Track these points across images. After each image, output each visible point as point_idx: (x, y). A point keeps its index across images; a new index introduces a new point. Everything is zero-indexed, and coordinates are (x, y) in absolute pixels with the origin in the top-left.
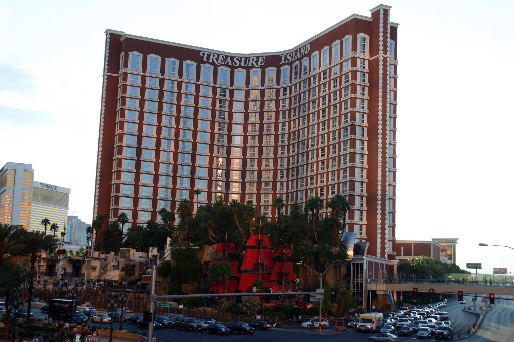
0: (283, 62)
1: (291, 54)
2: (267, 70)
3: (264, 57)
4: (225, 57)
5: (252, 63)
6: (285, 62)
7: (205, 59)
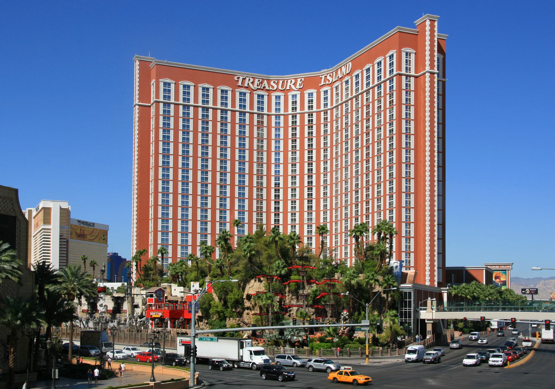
0: (322, 83)
1: (331, 74)
3: (303, 79)
4: (261, 80)
7: (240, 84)
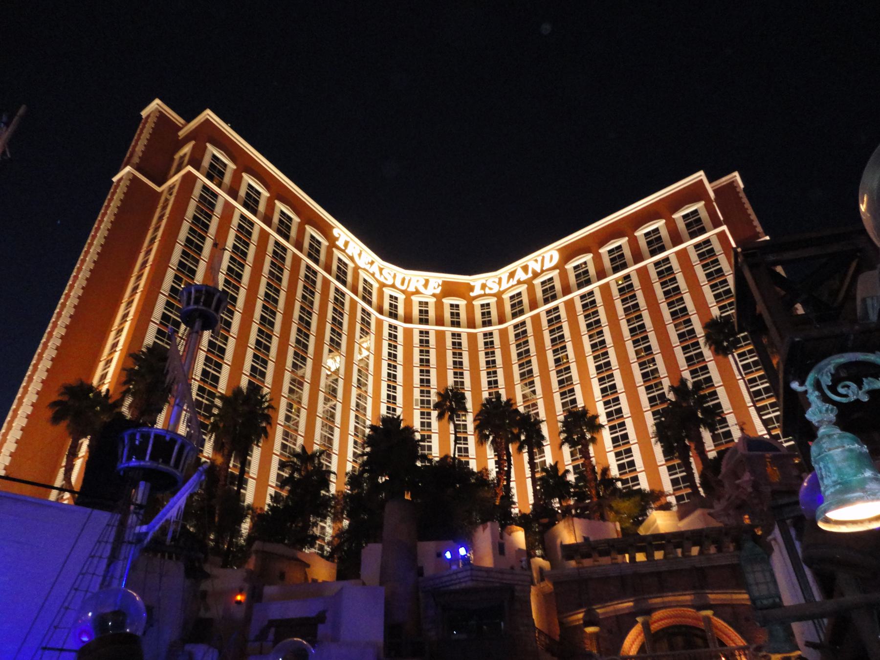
0: (477, 291)
2: (447, 301)
5: (416, 288)
6: (482, 292)
